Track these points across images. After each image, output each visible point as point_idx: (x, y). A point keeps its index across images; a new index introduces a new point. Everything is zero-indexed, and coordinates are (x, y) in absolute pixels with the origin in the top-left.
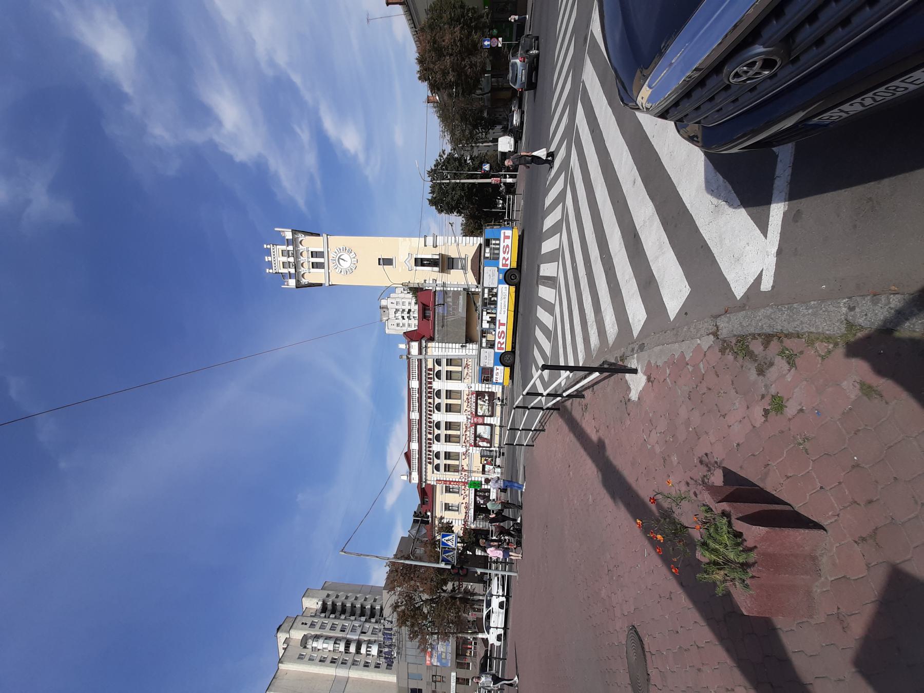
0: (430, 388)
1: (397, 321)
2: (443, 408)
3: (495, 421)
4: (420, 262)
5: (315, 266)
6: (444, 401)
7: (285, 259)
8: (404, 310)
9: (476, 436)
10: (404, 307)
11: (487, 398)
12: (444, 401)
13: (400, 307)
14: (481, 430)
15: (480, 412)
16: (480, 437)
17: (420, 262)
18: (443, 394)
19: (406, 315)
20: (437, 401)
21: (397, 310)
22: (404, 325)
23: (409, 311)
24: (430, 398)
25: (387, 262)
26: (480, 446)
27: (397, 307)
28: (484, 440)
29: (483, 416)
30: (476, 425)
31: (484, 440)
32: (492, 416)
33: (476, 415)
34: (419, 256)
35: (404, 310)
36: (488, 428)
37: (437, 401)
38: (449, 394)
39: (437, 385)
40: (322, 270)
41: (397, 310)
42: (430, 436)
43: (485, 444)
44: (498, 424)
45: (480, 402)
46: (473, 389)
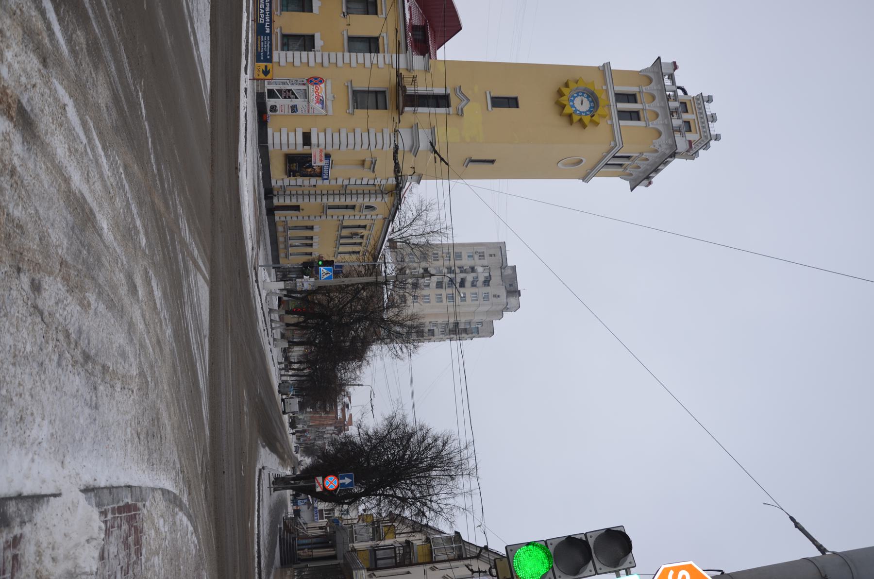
1: (485, 262)
4: (442, 101)
5: (631, 98)
7: (686, 117)
8: (473, 285)
10: (474, 290)
13: (482, 290)
17: (442, 101)
19: (470, 278)
21: (487, 282)
23: (462, 284)
25: (500, 102)
27: (487, 289)
34: (442, 110)
35: (473, 285)
41: (487, 282)
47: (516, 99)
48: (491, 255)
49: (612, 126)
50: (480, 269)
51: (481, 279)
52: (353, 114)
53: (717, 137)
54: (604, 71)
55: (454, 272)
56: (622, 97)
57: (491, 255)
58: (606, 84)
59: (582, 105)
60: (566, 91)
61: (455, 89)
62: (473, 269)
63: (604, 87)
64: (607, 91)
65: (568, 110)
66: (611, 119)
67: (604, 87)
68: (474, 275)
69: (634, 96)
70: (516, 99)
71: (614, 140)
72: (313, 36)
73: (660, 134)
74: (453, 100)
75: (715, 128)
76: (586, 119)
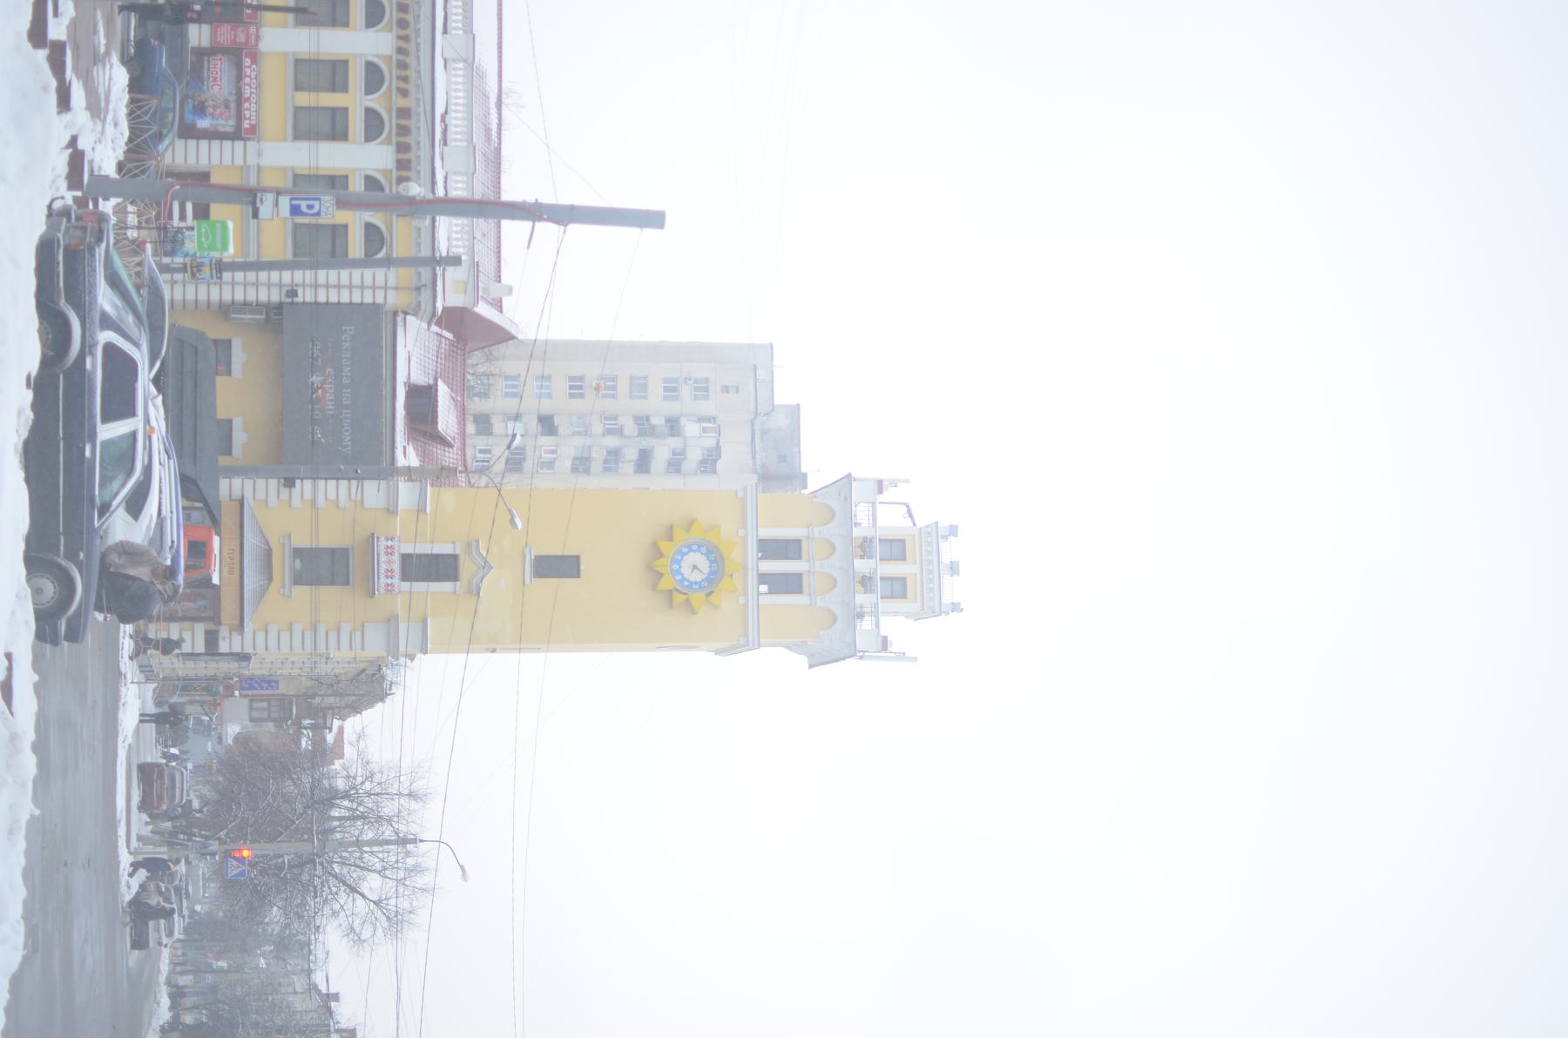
0: (402, 148)
1: (706, 407)
2: (356, 77)
5: (788, 549)
6: (355, 100)
12: (355, 100)
18: (356, 124)
20: (375, 101)
22: (671, 390)
23: (643, 463)
24: (404, 113)
34: (446, 586)
35: (675, 466)
37: (375, 101)
38: (334, 128)
39: (375, 157)
40: (765, 533)
41: (709, 463)
46: (252, 145)
47: (577, 558)
48: (726, 389)
49: (746, 606)
50: (691, 429)
51: (694, 456)
52: (290, 596)
53: (956, 607)
54: (744, 500)
55: (619, 432)
56: (770, 549)
57: (726, 389)
58: (745, 527)
59: (694, 566)
60: (665, 546)
61: (469, 545)
62: (674, 427)
63: (741, 532)
64: (745, 538)
65: (665, 584)
66: (745, 593)
67: (741, 532)
68: (675, 442)
69: (798, 542)
70: (577, 558)
71: (746, 635)
72: (230, 421)
73: (834, 619)
74: (466, 568)
75: (952, 589)
76: (697, 598)
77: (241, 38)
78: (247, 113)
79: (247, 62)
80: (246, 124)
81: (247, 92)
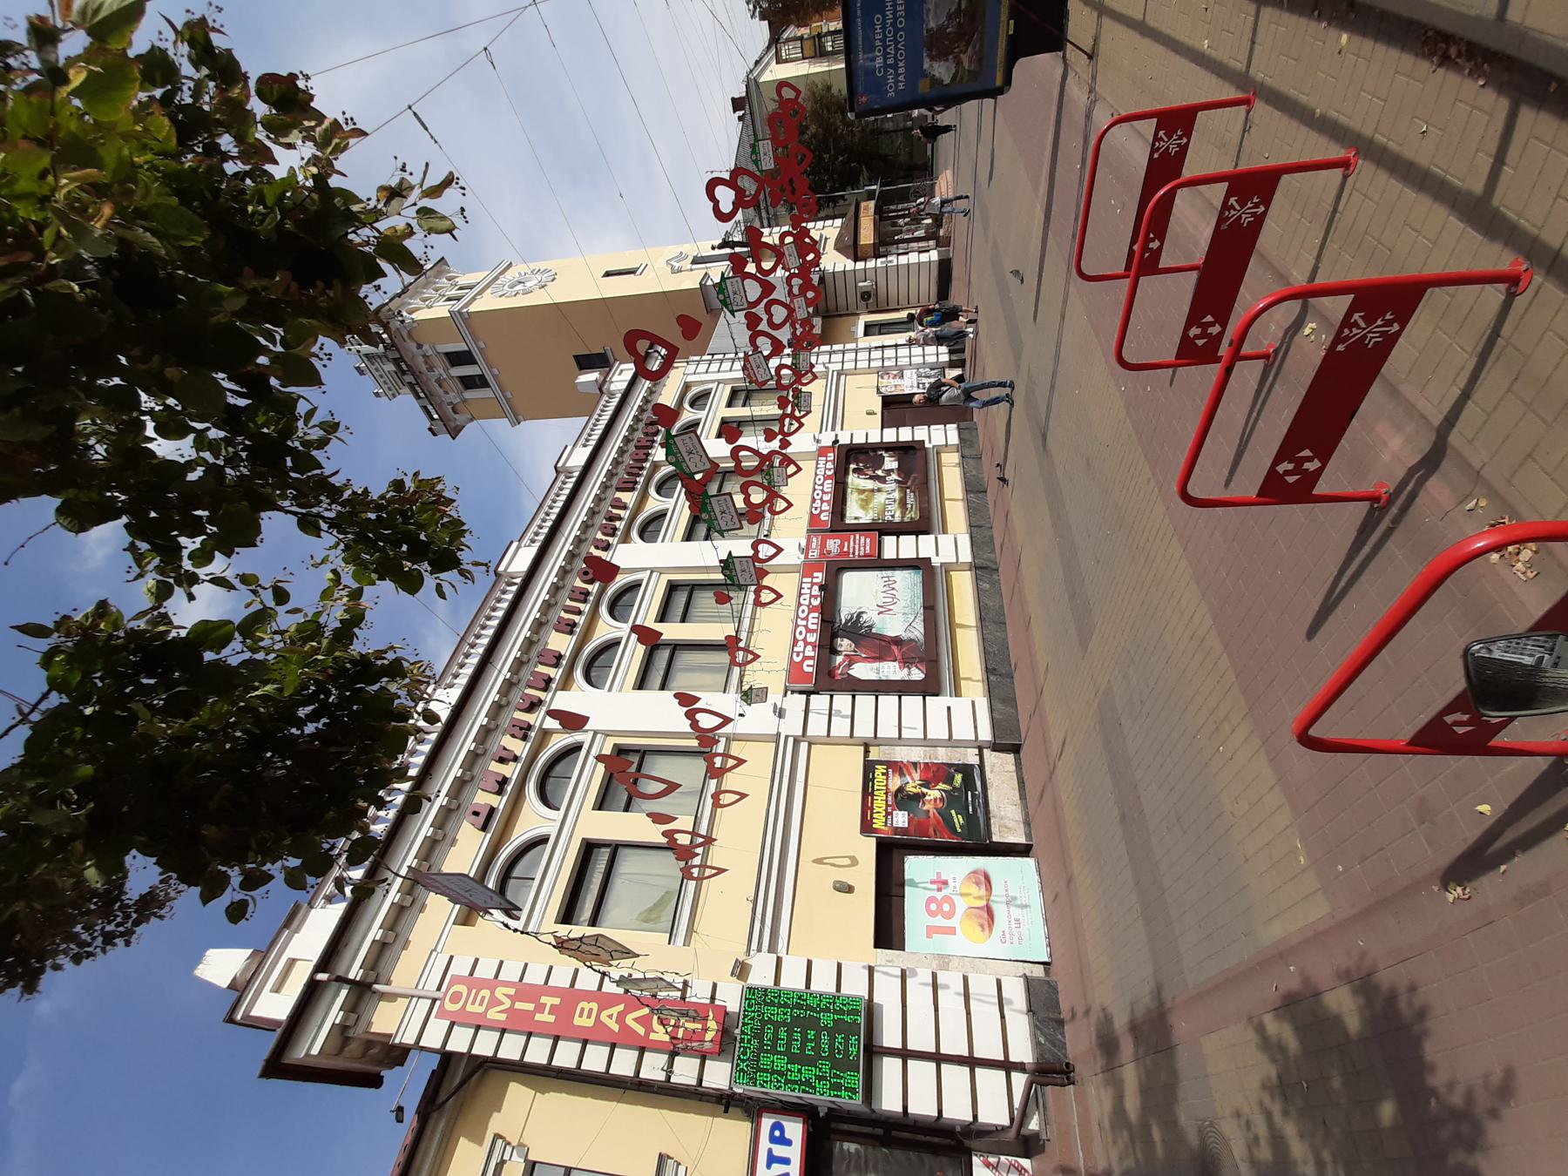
3: (950, 545)
9: (833, 627)
11: (890, 463)
14: (860, 593)
15: (855, 512)
16: (858, 631)
26: (856, 687)
28: (883, 647)
29: (883, 529)
30: (836, 569)
31: (883, 647)
32: (920, 527)
33: (839, 524)
36: (907, 583)
42: (560, 643)
43: (891, 671)
44: (966, 556)
45: (853, 480)
77: (833, 545)
78: (830, 465)
79: (825, 517)
80: (831, 456)
81: (829, 486)
